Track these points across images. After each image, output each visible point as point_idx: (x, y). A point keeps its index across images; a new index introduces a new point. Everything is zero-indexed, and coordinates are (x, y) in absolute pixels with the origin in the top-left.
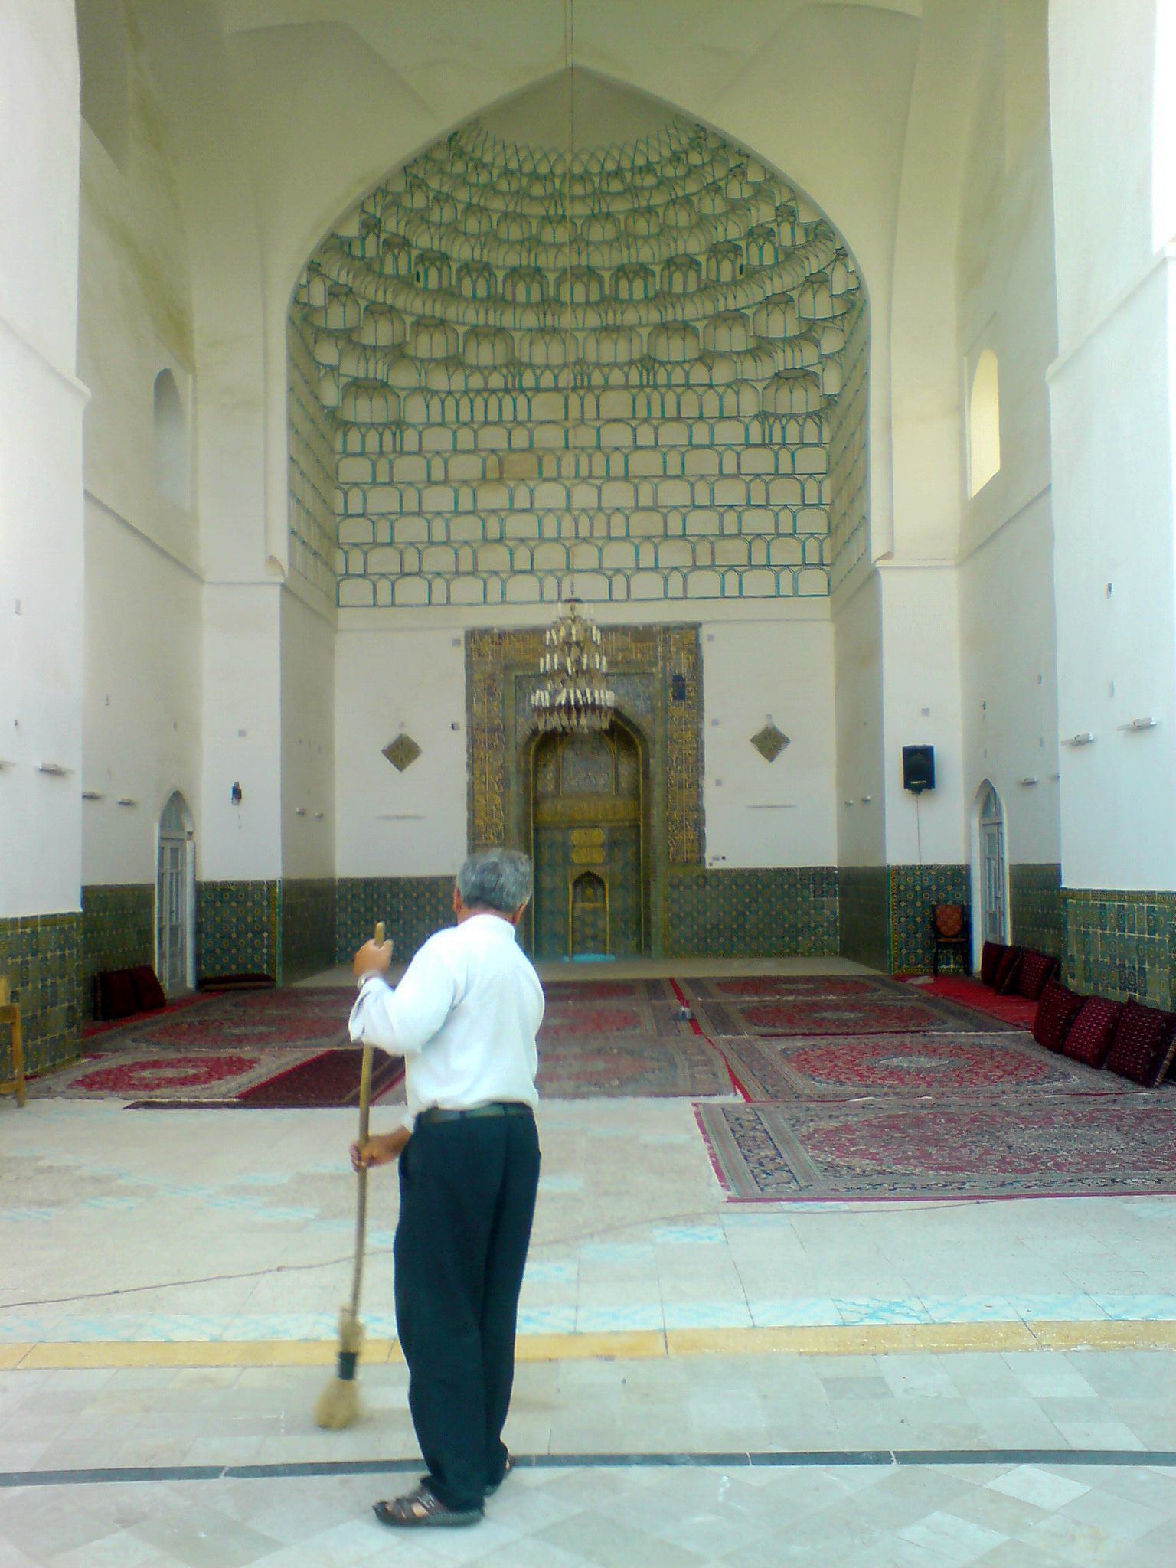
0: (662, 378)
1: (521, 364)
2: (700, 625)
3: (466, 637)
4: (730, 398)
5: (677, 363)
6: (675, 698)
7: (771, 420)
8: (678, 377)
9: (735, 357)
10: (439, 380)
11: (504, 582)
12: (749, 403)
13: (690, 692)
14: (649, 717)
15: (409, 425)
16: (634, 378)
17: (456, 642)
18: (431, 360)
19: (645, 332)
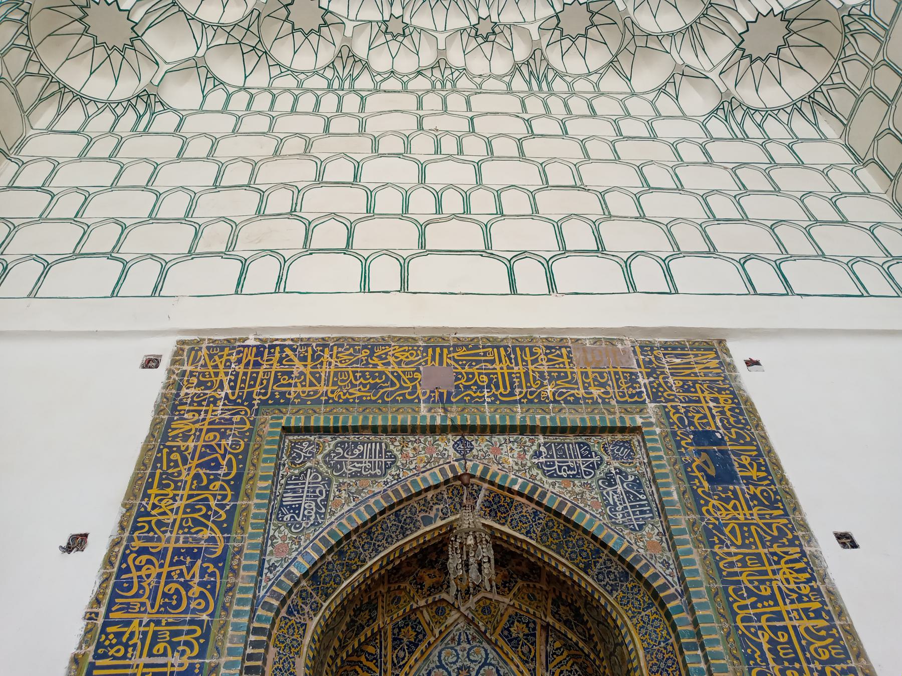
0: (559, 85)
1: (356, 60)
2: (720, 342)
3: (178, 353)
4: (665, 104)
5: (580, 75)
6: (710, 479)
7: (739, 114)
8: (581, 85)
9: (666, 44)
10: (229, 70)
11: (285, 264)
12: (697, 101)
13: (742, 463)
14: (652, 532)
15: (166, 108)
16: (518, 83)
17: (151, 363)
18: (220, 26)
19: (534, 29)
